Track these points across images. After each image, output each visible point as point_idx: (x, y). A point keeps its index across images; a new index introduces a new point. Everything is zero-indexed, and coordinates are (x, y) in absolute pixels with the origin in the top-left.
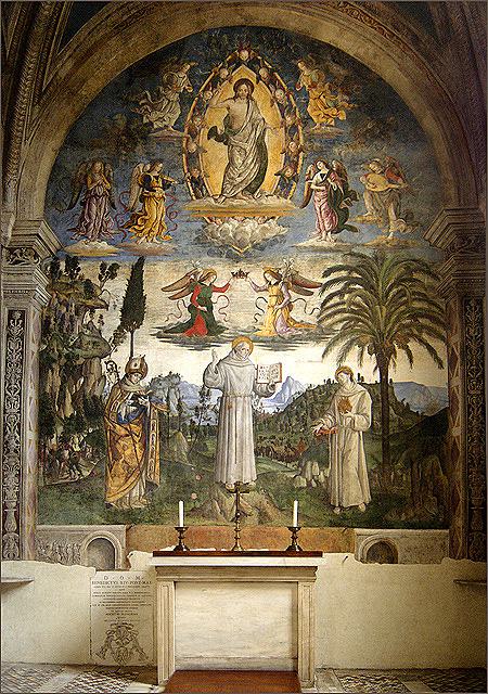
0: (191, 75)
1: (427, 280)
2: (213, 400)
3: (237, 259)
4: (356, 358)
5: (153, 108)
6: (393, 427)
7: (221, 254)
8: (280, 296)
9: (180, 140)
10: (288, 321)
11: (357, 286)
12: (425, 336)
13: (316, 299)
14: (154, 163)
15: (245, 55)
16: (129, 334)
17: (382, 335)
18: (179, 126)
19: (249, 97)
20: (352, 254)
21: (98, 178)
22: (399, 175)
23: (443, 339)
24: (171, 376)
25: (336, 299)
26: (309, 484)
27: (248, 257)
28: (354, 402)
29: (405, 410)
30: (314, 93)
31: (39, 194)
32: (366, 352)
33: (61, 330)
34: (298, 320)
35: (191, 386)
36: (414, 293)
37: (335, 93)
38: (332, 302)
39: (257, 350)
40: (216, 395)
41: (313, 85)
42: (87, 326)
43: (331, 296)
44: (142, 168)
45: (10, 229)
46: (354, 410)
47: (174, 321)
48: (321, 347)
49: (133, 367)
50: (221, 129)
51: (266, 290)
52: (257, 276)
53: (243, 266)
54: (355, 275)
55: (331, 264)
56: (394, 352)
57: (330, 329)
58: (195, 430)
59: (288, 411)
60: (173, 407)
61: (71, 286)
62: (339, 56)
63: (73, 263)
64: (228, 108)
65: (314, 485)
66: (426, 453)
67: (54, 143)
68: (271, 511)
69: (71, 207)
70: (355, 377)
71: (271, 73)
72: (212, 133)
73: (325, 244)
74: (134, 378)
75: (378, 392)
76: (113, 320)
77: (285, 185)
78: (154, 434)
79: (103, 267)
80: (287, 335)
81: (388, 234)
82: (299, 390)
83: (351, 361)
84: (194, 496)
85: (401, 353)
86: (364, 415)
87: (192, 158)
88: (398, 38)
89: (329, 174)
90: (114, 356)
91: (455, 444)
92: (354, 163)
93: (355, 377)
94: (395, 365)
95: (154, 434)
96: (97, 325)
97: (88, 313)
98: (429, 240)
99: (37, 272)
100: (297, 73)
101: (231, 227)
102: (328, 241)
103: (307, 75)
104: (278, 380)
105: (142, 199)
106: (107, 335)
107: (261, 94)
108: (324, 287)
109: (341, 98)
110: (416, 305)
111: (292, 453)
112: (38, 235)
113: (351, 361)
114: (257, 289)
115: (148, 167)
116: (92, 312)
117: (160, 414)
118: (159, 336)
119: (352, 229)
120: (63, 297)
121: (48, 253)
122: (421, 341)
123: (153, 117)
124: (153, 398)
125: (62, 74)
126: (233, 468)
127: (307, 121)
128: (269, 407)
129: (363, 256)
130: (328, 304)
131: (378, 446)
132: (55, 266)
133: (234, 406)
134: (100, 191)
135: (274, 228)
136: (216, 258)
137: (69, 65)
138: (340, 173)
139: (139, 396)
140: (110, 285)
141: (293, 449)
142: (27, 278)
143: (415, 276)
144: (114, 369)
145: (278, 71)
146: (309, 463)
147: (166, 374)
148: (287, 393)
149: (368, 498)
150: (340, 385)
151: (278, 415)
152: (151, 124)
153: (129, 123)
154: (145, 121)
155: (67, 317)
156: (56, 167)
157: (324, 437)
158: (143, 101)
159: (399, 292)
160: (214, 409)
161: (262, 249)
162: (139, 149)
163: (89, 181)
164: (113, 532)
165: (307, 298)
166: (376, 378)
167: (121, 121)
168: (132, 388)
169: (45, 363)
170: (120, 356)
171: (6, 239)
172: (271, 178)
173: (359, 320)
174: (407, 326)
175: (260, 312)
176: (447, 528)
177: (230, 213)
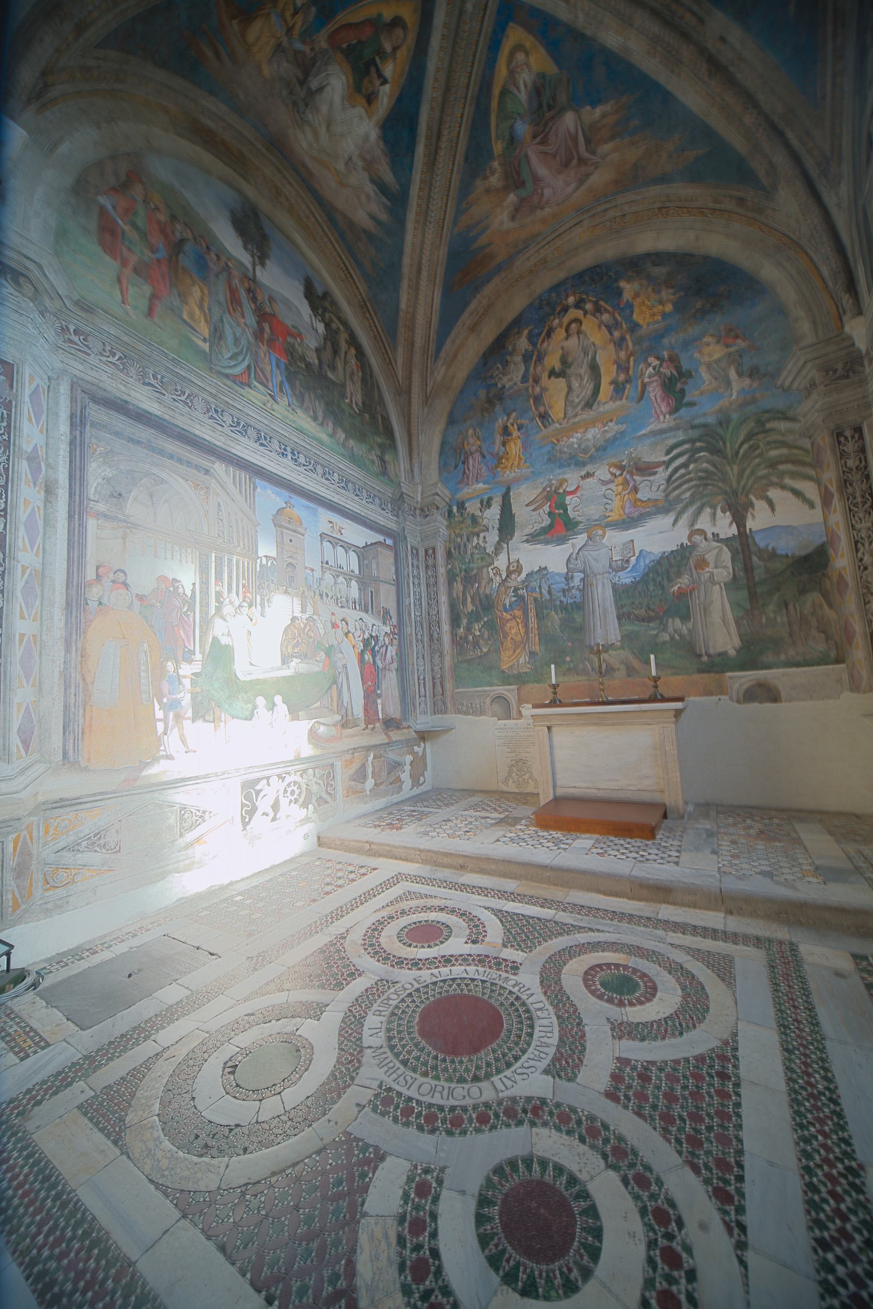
0: (530, 338)
1: (782, 425)
2: (577, 581)
3: (584, 464)
4: (709, 520)
5: (504, 374)
6: (759, 574)
7: (569, 465)
8: (626, 483)
9: (527, 389)
10: (636, 502)
11: (702, 454)
12: (787, 481)
13: (662, 474)
14: (509, 415)
15: (571, 300)
16: (505, 546)
17: (735, 493)
18: (525, 379)
19: (579, 332)
20: (693, 427)
21: (471, 440)
22: (737, 337)
23: (809, 478)
24: (541, 569)
25: (682, 471)
26: (672, 638)
27: (592, 459)
28: (710, 557)
29: (773, 555)
30: (639, 300)
31: (434, 466)
32: (719, 511)
33: (459, 553)
34: (645, 499)
35: (558, 574)
36: (769, 443)
37: (657, 291)
38: (677, 475)
39: (609, 533)
40: (578, 576)
41: (637, 295)
42: (476, 547)
43: (676, 470)
44: (500, 422)
45: (419, 495)
46: (712, 565)
47: (537, 527)
48: (671, 518)
49: (511, 568)
50: (558, 367)
51: (613, 482)
52: (603, 472)
53: (589, 468)
54: (698, 444)
55: (671, 442)
56: (752, 505)
57: (678, 499)
58: (564, 608)
59: (645, 579)
60: (545, 592)
61: (462, 522)
62: (657, 258)
63: (461, 506)
64: (562, 348)
65: (677, 637)
66: (803, 592)
67: (440, 427)
68: (636, 664)
69: (456, 467)
70: (710, 536)
71: (596, 304)
72: (552, 373)
73: (664, 426)
74: (513, 576)
75: (737, 544)
76: (493, 537)
77: (619, 389)
78: (532, 615)
79: (482, 502)
80: (636, 515)
81: (731, 395)
82: (653, 558)
83: (704, 523)
84: (568, 659)
85: (760, 505)
86: (725, 567)
87: (538, 399)
88: (720, 210)
89: (661, 365)
90: (496, 564)
91: (841, 576)
92: (686, 345)
93: (710, 536)
94: (753, 517)
95: (532, 615)
96: (482, 545)
97: (475, 538)
98: (782, 386)
99: (439, 518)
100: (619, 292)
101: (575, 440)
102: (668, 421)
103: (628, 288)
104: (631, 554)
105: (504, 444)
106: (490, 549)
107: (589, 325)
108: (668, 464)
109: (666, 294)
110: (774, 453)
111: (652, 614)
112: (438, 494)
113: (704, 523)
114: (604, 483)
115: (505, 418)
116: (478, 536)
117: (536, 600)
118: (527, 541)
119: (691, 404)
120: (457, 531)
121: (444, 504)
122: (783, 487)
123: (505, 379)
124: (529, 589)
125: (439, 378)
126: (599, 631)
127: (635, 327)
128: (625, 578)
129: (705, 426)
130: (674, 478)
131: (745, 593)
132: (450, 512)
133: (595, 582)
134: (474, 448)
135: (613, 428)
136: (566, 469)
137: (443, 371)
138: (673, 360)
139: (519, 589)
140: (488, 513)
141: (653, 611)
142: (433, 524)
143: (768, 426)
144: (498, 572)
145: (602, 299)
146: (670, 621)
147: (536, 569)
148: (642, 564)
149: (737, 642)
150: (694, 546)
151: (635, 584)
152: (504, 387)
153: (488, 393)
154: (499, 385)
155: (462, 545)
156: (443, 444)
157: (682, 594)
158: (497, 373)
159: (750, 447)
160: (578, 589)
161: (604, 449)
162: (498, 409)
163: (466, 444)
164: (508, 691)
165: (652, 478)
166: (734, 530)
167: (482, 393)
168: (512, 584)
169: (451, 579)
170: (501, 562)
171: (417, 502)
172: (606, 388)
173: (707, 485)
174: (764, 477)
175: (610, 502)
176: (838, 661)
177: (574, 428)
